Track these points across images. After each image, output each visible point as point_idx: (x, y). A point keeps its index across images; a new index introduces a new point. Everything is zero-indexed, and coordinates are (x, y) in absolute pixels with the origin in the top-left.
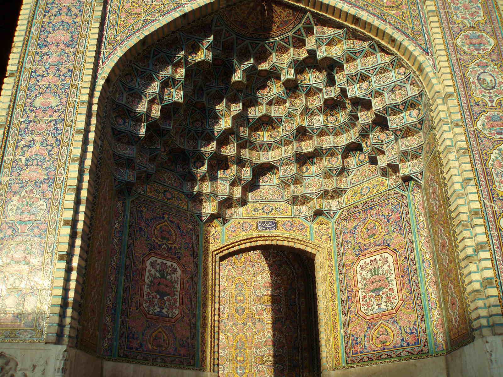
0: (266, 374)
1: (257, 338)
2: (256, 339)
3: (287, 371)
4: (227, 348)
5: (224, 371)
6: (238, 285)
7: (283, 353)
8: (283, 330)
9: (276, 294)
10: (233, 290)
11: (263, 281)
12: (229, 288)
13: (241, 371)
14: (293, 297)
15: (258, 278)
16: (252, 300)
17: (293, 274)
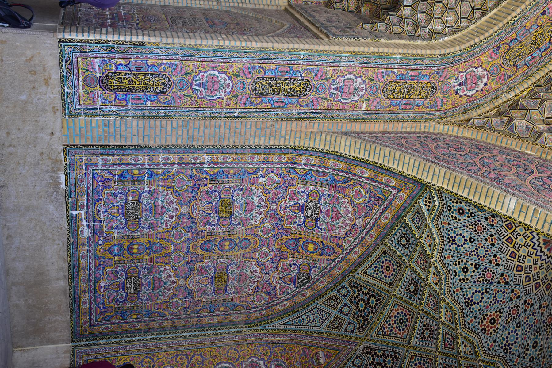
0: (112, 282)
1: (165, 269)
2: (163, 268)
3: (116, 306)
4: (152, 232)
5: (116, 228)
6: (247, 241)
7: (141, 299)
8: (175, 300)
9: (228, 289)
10: (240, 236)
11: (249, 273)
12: (244, 230)
13: (116, 251)
14: (222, 309)
15: (255, 266)
16: (222, 260)
17: (254, 308)
